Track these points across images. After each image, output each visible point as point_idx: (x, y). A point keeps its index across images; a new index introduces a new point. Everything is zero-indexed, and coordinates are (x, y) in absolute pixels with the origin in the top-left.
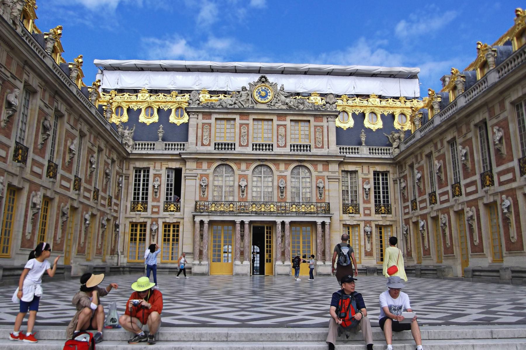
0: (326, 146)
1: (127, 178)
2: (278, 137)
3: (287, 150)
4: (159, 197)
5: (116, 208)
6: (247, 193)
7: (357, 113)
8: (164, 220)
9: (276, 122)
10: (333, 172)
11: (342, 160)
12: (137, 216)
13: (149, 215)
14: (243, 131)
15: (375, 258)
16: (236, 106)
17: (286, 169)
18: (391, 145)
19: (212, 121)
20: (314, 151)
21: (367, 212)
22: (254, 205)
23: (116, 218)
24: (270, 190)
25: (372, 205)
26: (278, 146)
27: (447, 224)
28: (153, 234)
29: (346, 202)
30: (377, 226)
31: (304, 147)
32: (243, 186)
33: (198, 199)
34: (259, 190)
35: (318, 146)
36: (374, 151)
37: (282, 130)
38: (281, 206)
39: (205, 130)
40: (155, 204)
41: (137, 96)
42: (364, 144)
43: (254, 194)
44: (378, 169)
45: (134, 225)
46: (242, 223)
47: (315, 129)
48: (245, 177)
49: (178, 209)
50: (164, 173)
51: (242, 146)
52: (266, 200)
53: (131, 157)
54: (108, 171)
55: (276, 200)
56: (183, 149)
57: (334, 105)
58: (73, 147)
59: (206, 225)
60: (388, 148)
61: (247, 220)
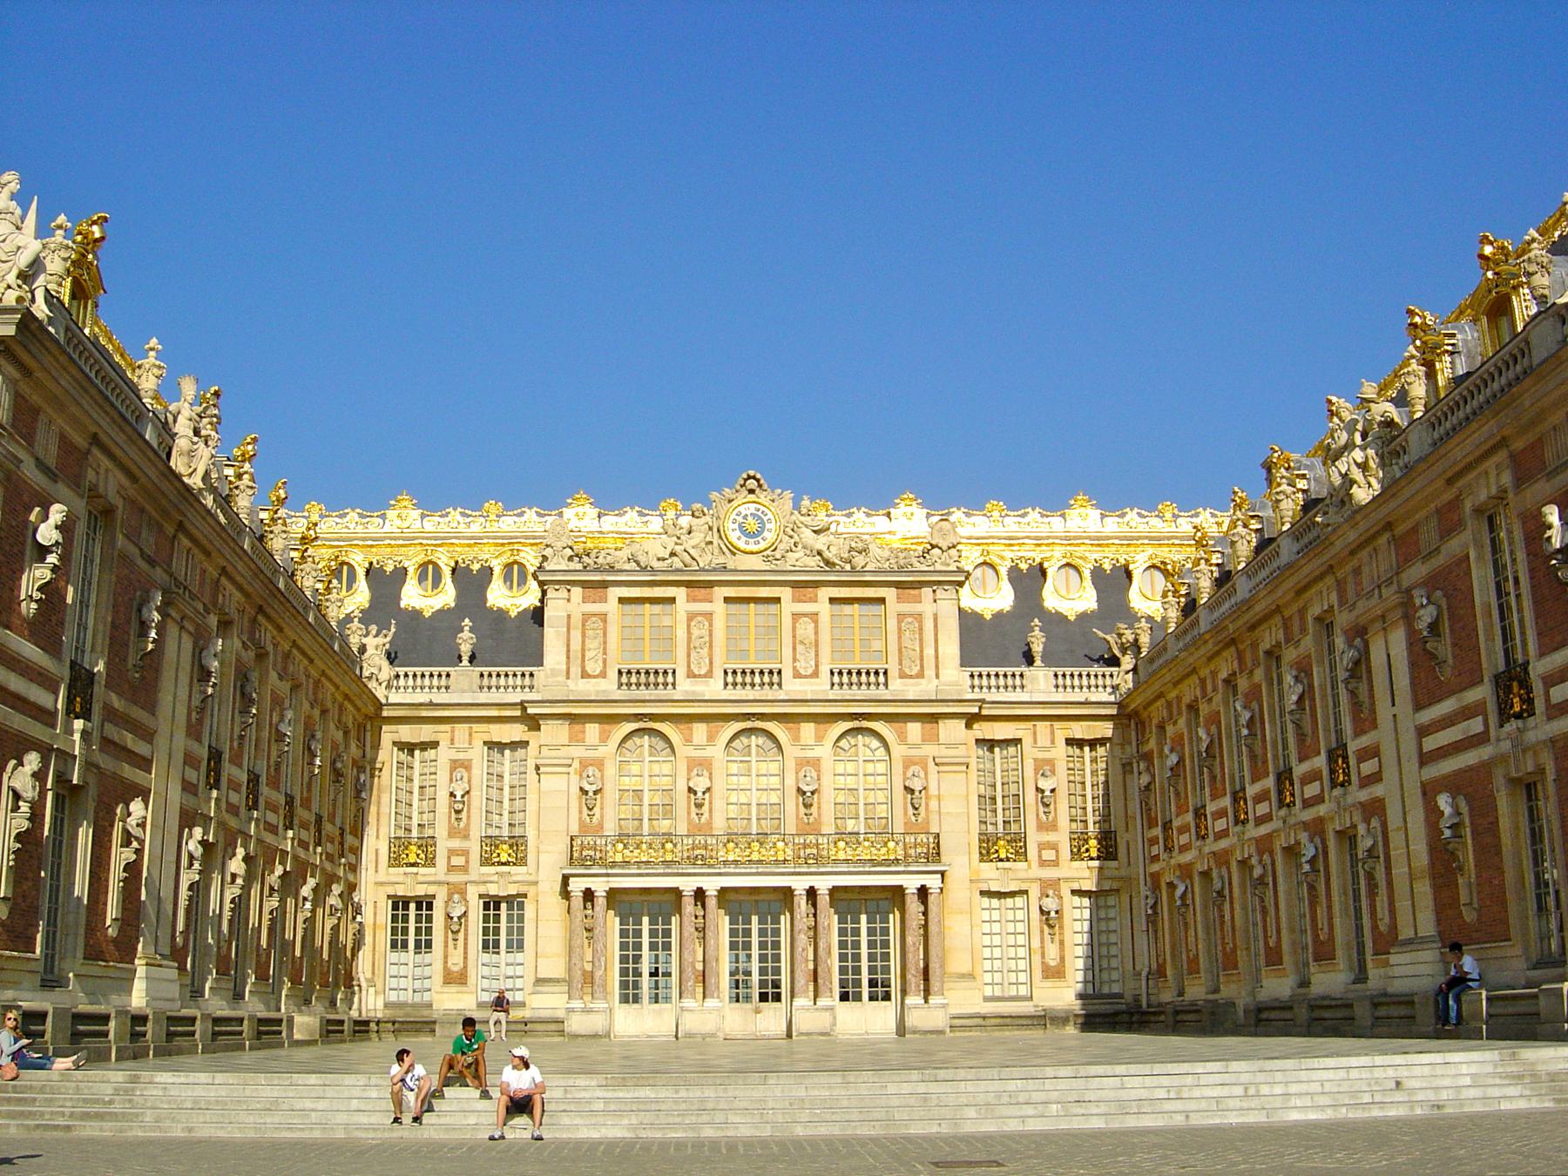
0: (930, 672)
2: (794, 649)
3: (820, 687)
4: (468, 824)
5: (352, 859)
6: (711, 811)
7: (1024, 566)
8: (482, 889)
9: (789, 606)
10: (949, 746)
11: (976, 710)
12: (409, 880)
13: (442, 877)
14: (695, 632)
15: (1072, 983)
17: (819, 738)
19: (611, 606)
20: (897, 687)
21: (1049, 855)
22: (731, 845)
24: (774, 798)
26: (797, 675)
27: (1226, 892)
28: (455, 927)
29: (991, 829)
30: (1074, 892)
31: (868, 673)
32: (700, 790)
33: (575, 830)
34: (743, 799)
35: (907, 671)
36: (1068, 682)
37: (806, 628)
38: (805, 846)
39: (590, 633)
40: (456, 843)
41: (383, 516)
42: (1038, 662)
43: (733, 811)
44: (1079, 730)
45: (400, 903)
46: (700, 894)
47: (899, 622)
48: (704, 765)
50: (478, 754)
51: (695, 676)
52: (767, 826)
53: (385, 714)
54: (339, 765)
56: (532, 687)
57: (953, 552)
59: (601, 902)
60: (1108, 670)
61: (712, 885)
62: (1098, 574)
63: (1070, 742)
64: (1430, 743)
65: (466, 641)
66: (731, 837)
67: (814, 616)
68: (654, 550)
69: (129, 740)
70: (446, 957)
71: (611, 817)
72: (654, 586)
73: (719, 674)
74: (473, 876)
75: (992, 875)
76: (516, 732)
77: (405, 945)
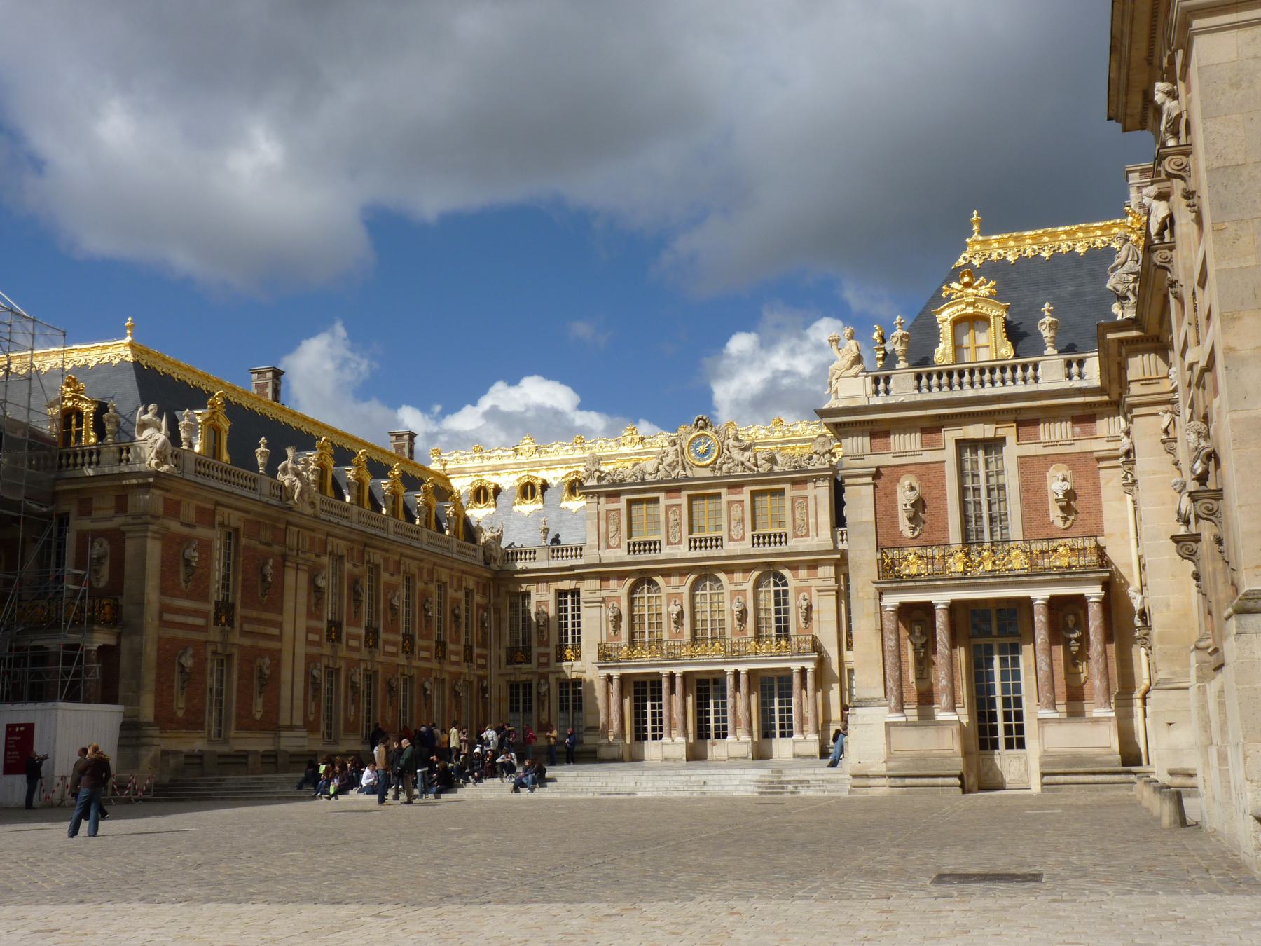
0: (812, 533)
1: (498, 611)
2: (730, 523)
3: (745, 547)
10: (825, 579)
13: (535, 670)
14: (672, 517)
16: (659, 476)
26: (731, 539)
40: (542, 650)
45: (514, 687)
46: (672, 676)
50: (551, 598)
58: (395, 602)
59: (615, 682)
61: (678, 671)
69: (262, 629)
70: (539, 716)
73: (685, 541)
74: (552, 669)
77: (518, 710)
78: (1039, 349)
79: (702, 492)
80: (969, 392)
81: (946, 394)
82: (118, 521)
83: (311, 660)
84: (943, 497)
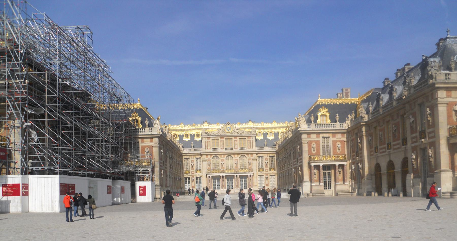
3: (238, 150)
9: (233, 139)
18: (276, 146)
23: (180, 176)
25: (268, 168)
37: (236, 142)
44: (271, 155)
46: (223, 176)
48: (223, 160)
49: (201, 172)
50: (195, 159)
55: (234, 168)
61: (224, 175)
62: (275, 133)
63: (270, 156)
64: (295, 163)
65: (192, 145)
66: (227, 169)
67: (237, 141)
68: (216, 132)
71: (211, 167)
72: (216, 137)
75: (260, 173)
76: (199, 156)
78: (336, 122)
79: (229, 138)
80: (324, 129)
81: (320, 129)
82: (151, 144)
83: (170, 172)
84: (319, 147)
